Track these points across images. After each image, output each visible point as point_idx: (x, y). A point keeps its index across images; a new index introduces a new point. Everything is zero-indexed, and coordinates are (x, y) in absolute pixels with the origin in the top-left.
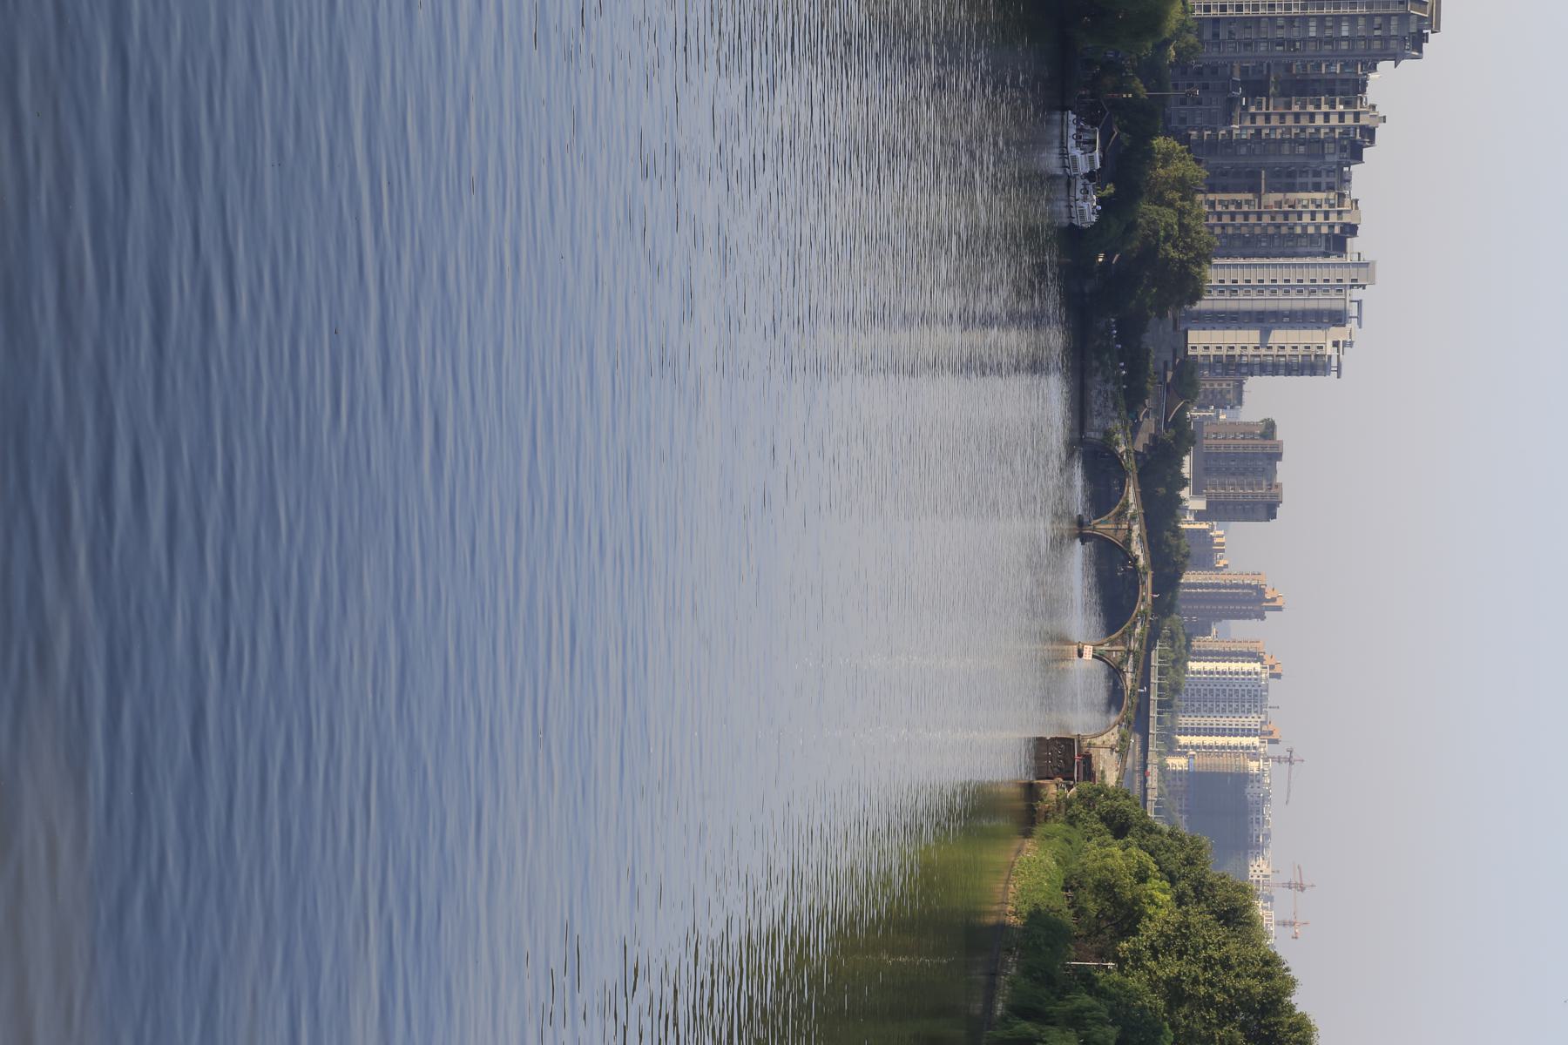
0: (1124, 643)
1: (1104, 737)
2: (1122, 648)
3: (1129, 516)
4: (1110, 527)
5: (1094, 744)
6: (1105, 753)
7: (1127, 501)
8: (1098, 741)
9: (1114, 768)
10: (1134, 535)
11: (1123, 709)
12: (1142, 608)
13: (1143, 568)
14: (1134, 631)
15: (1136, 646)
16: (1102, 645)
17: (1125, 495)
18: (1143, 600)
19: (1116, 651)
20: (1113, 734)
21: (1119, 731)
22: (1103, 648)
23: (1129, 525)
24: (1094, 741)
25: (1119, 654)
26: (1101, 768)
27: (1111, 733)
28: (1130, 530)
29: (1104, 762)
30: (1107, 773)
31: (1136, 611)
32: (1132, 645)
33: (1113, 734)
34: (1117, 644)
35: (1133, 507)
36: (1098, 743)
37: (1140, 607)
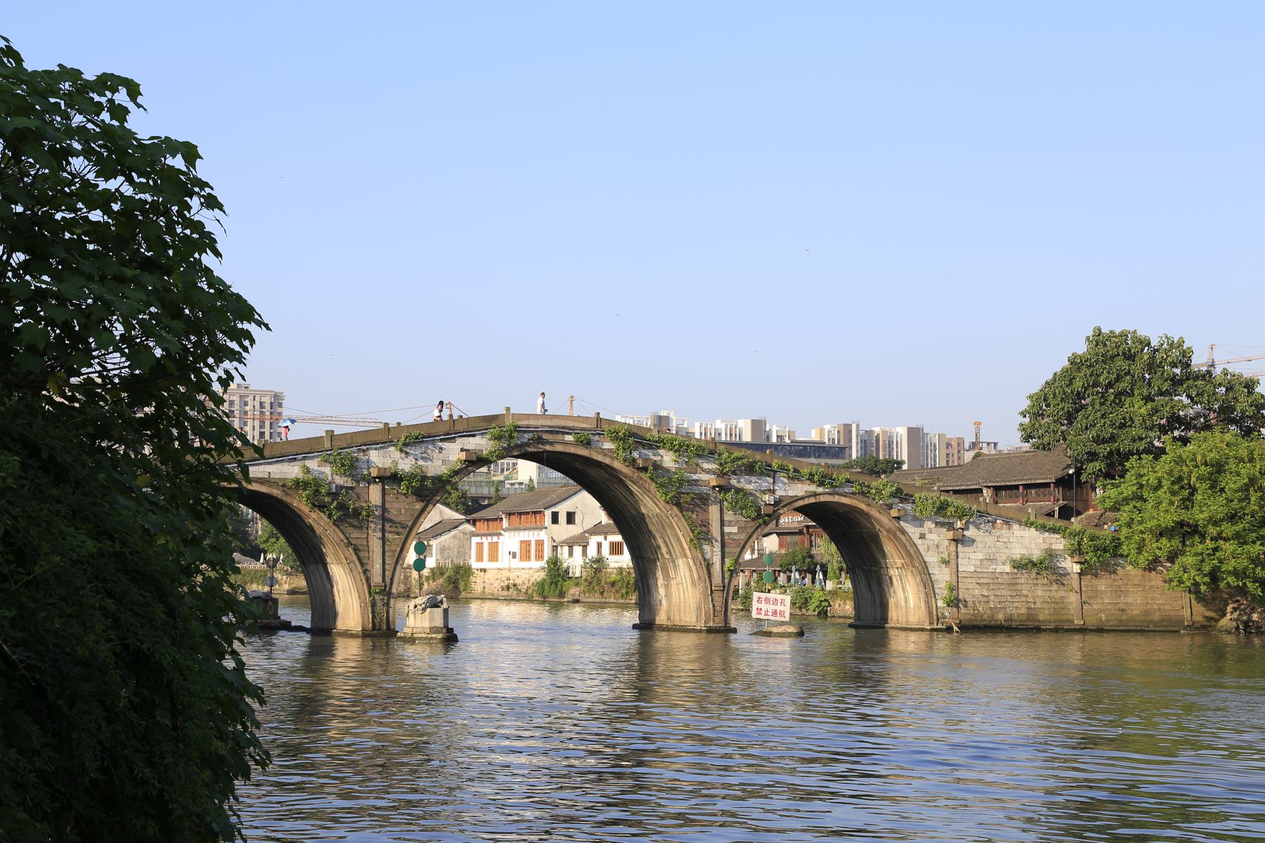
0: (703, 500)
1: (932, 559)
2: (714, 511)
3: (340, 481)
4: (376, 545)
5: (951, 589)
6: (970, 560)
7: (298, 484)
8: (942, 576)
9: (1004, 531)
10: (406, 465)
11: (863, 507)
12: (608, 445)
13: (498, 438)
14: (667, 470)
15: (706, 466)
16: (709, 566)
17: (276, 492)
18: (588, 444)
19: (722, 523)
20: (922, 536)
21: (918, 521)
22: (717, 560)
23: (371, 480)
24: (942, 590)
25: (729, 516)
26: (1008, 569)
27: (919, 542)
28: (391, 478)
29: (992, 560)
30: (1018, 552)
31: (617, 465)
32: (705, 477)
33: (922, 536)
34: (705, 524)
35: (313, 464)
36: (948, 578)
37: (605, 453)
